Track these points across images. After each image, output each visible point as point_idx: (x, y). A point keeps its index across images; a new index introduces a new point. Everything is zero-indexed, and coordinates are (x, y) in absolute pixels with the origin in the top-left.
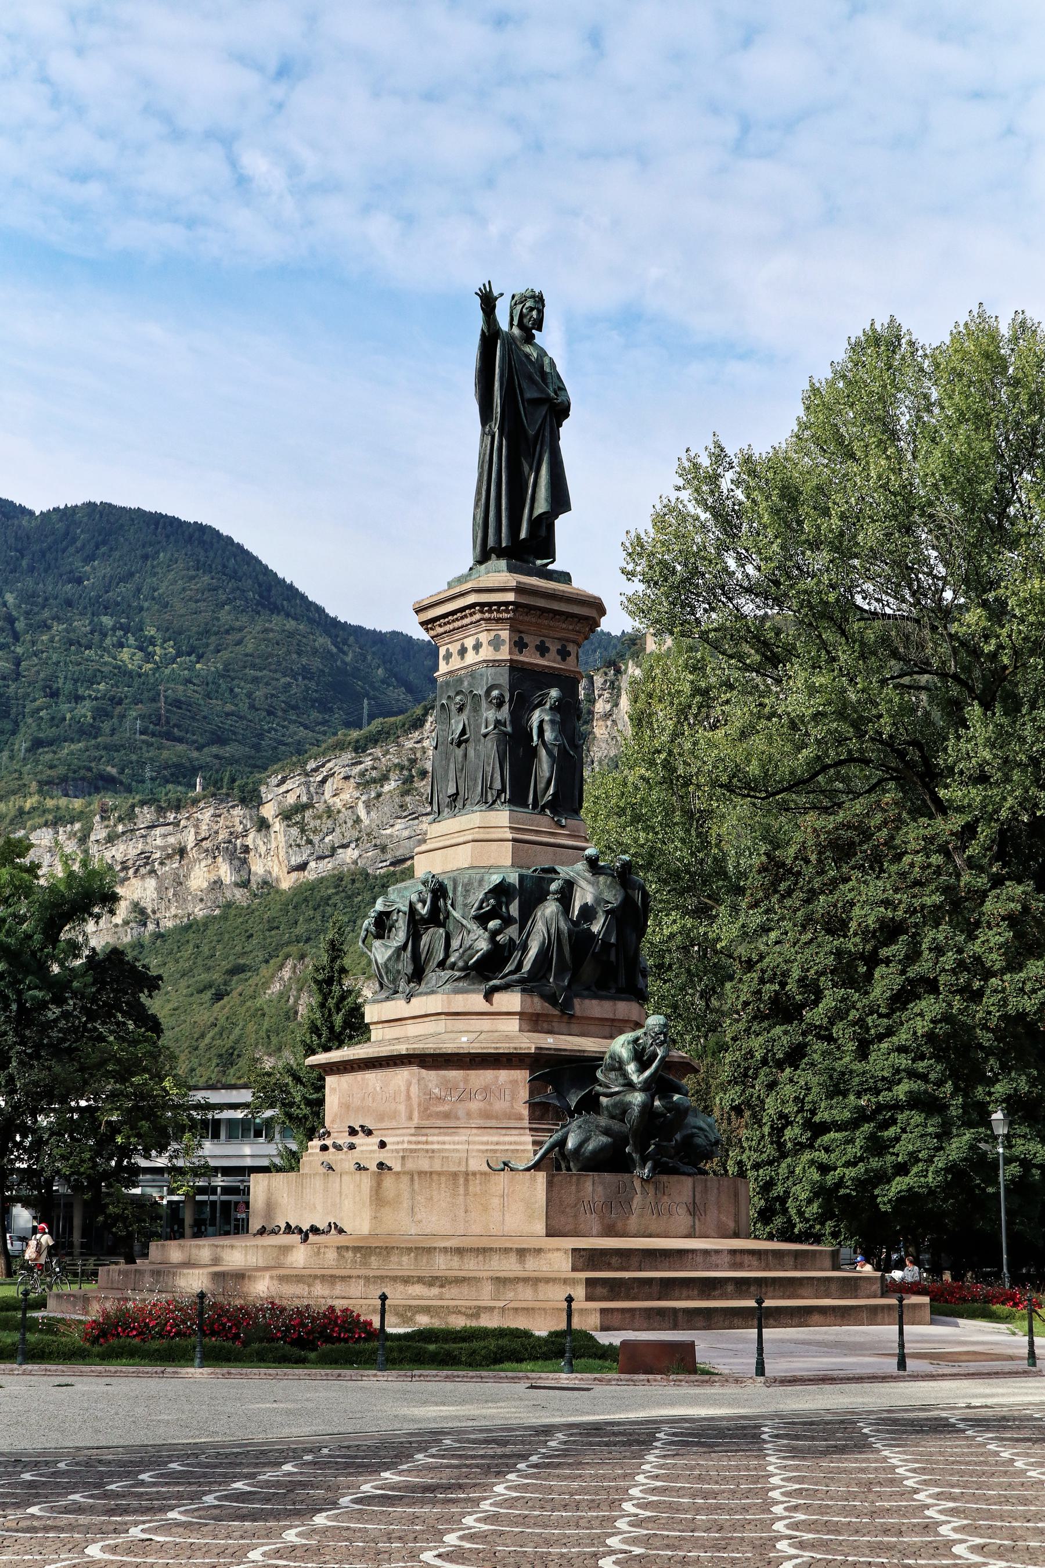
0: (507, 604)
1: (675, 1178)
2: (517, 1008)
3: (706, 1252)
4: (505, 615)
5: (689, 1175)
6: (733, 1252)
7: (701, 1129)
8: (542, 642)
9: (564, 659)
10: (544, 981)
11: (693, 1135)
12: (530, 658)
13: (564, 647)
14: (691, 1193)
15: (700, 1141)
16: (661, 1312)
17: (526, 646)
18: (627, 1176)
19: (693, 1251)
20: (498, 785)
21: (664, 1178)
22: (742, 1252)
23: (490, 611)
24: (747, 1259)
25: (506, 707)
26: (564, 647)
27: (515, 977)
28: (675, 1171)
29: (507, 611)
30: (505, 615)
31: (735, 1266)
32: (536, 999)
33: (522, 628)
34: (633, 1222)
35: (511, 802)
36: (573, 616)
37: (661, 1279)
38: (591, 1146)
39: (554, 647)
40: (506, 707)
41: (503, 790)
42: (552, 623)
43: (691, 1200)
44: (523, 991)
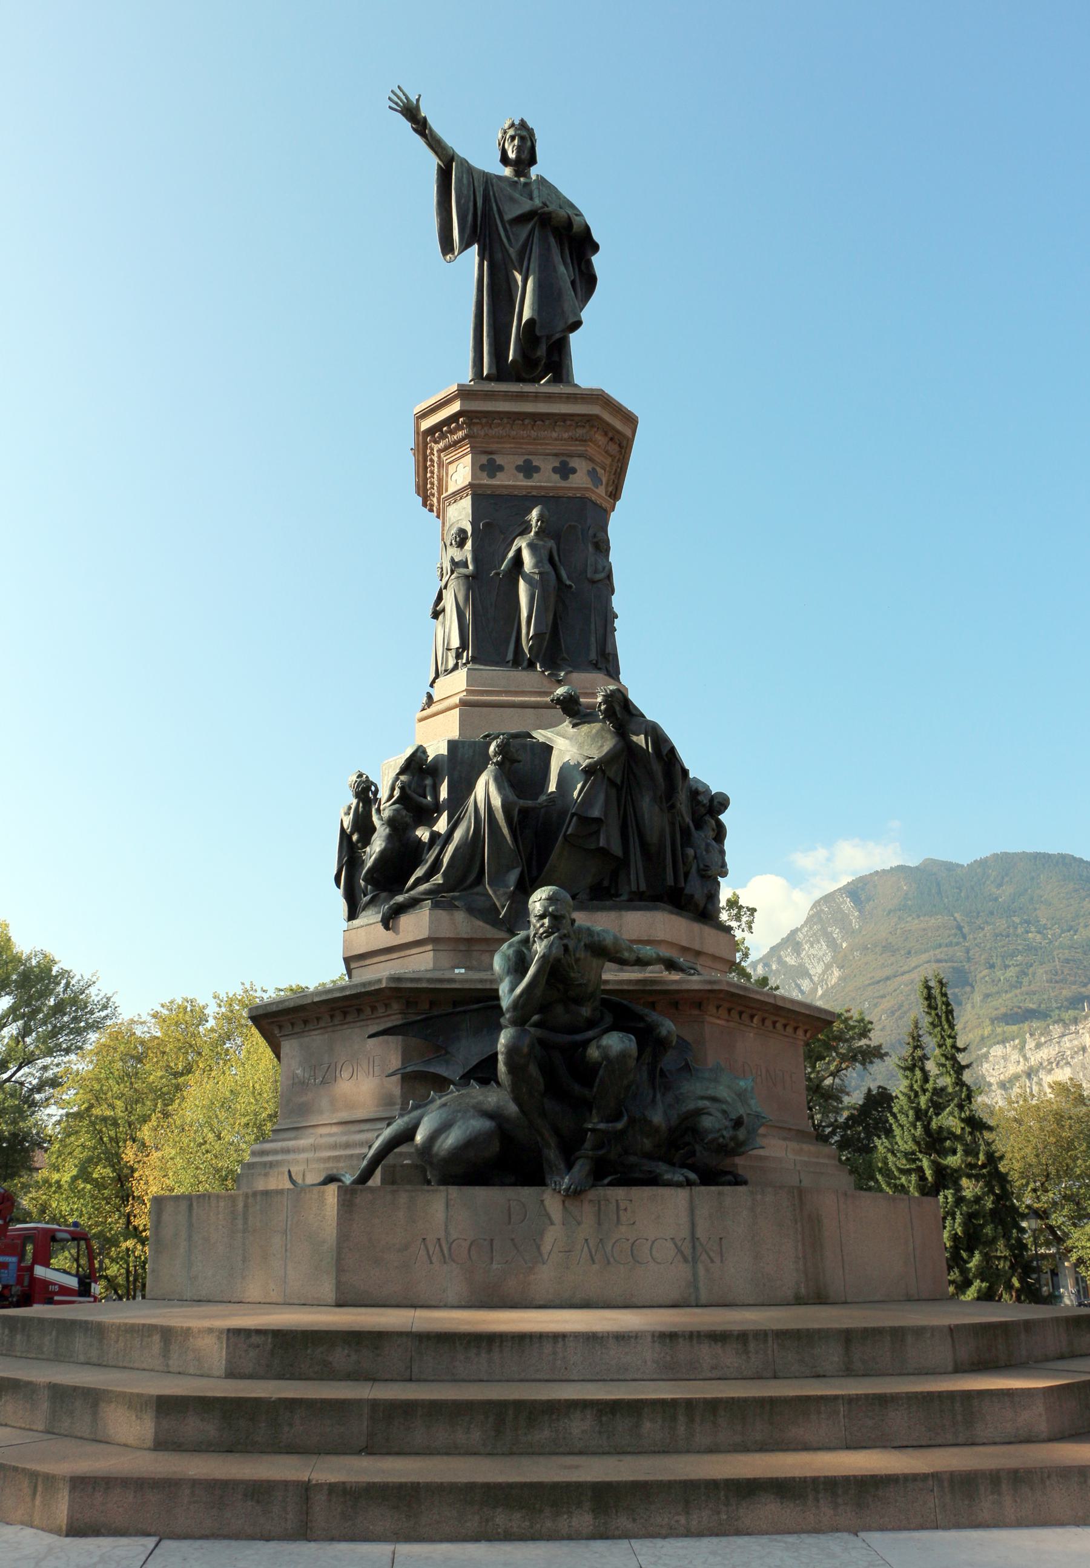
0: (454, 418)
1: (647, 1191)
2: (424, 934)
3: (592, 1339)
4: (461, 434)
5: (679, 1185)
6: (668, 1338)
7: (714, 1099)
8: (528, 462)
9: (565, 477)
10: (479, 889)
11: (699, 1112)
12: (509, 480)
13: (564, 464)
14: (684, 1219)
15: (707, 1122)
16: (259, 1492)
17: (500, 468)
18: (526, 1193)
19: (558, 1338)
20: (455, 643)
21: (620, 1192)
22: (694, 1337)
23: (443, 436)
24: (706, 1352)
25: (469, 545)
26: (564, 464)
27: (425, 887)
28: (653, 1181)
29: (459, 428)
30: (461, 434)
31: (670, 1372)
32: (460, 916)
33: (494, 447)
34: (545, 1278)
35: (474, 659)
36: (564, 417)
37: (374, 1404)
38: (450, 1140)
39: (546, 466)
40: (469, 545)
41: (464, 646)
42: (533, 434)
43: (685, 1232)
44: (436, 905)
